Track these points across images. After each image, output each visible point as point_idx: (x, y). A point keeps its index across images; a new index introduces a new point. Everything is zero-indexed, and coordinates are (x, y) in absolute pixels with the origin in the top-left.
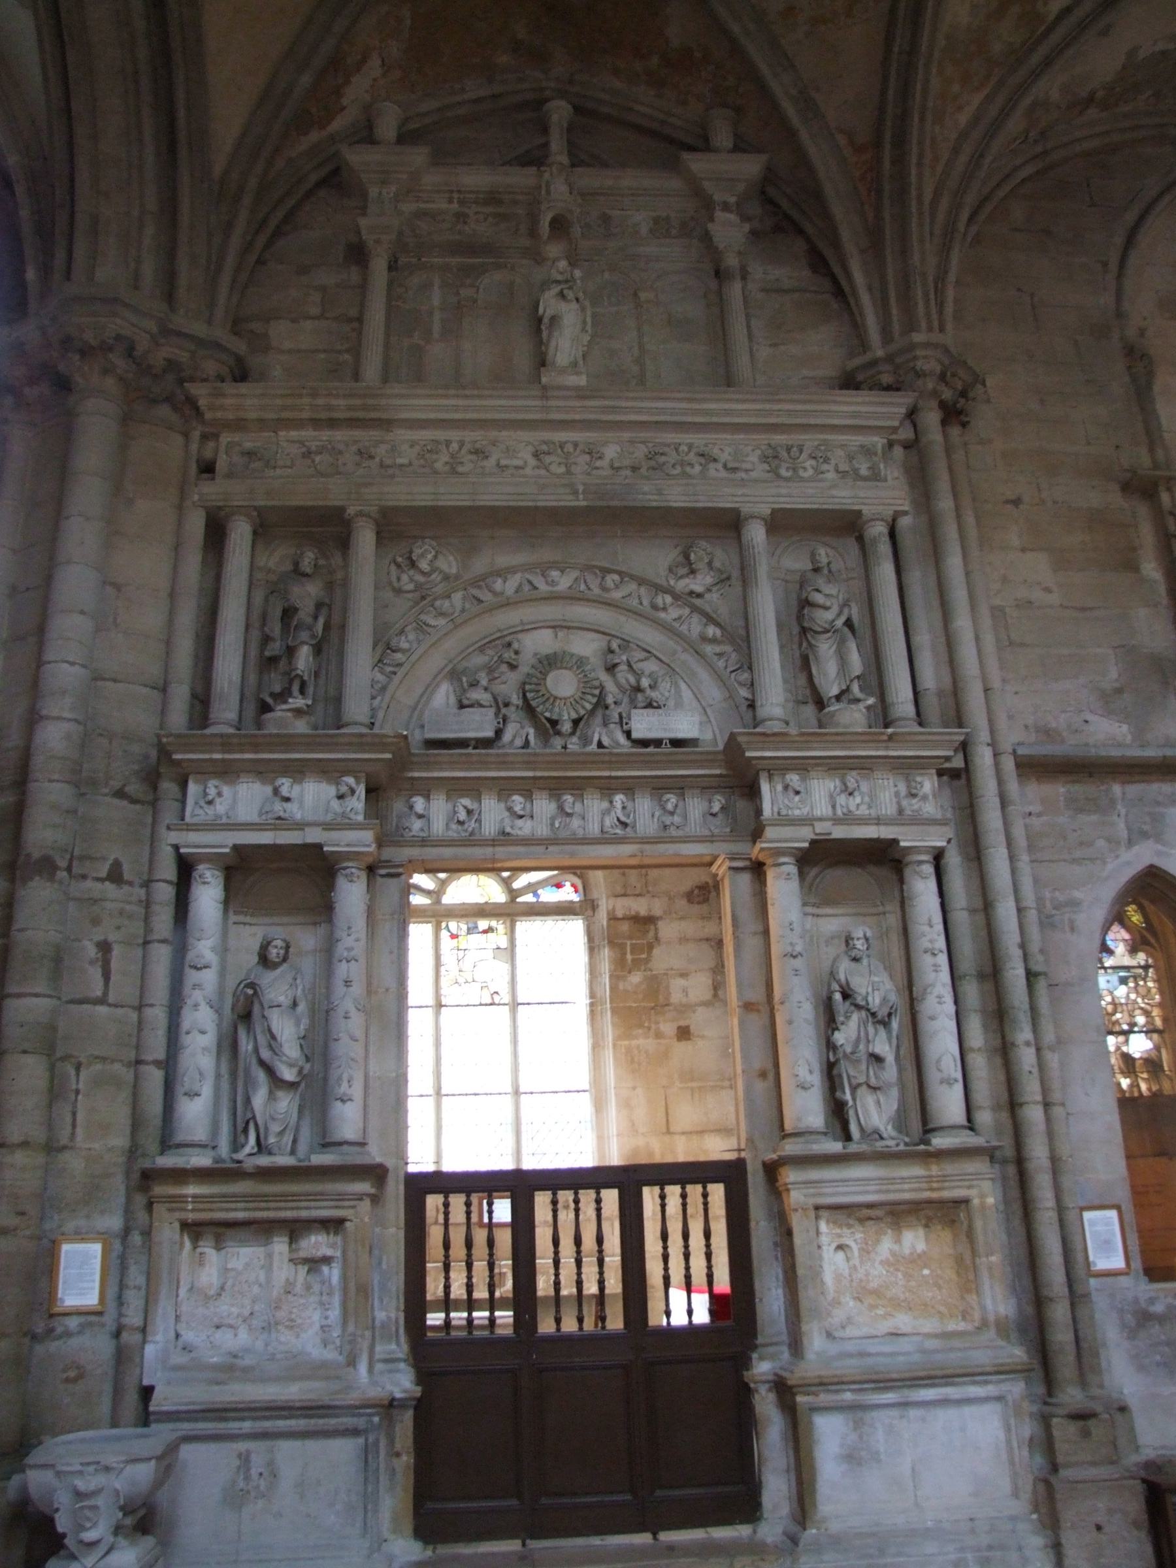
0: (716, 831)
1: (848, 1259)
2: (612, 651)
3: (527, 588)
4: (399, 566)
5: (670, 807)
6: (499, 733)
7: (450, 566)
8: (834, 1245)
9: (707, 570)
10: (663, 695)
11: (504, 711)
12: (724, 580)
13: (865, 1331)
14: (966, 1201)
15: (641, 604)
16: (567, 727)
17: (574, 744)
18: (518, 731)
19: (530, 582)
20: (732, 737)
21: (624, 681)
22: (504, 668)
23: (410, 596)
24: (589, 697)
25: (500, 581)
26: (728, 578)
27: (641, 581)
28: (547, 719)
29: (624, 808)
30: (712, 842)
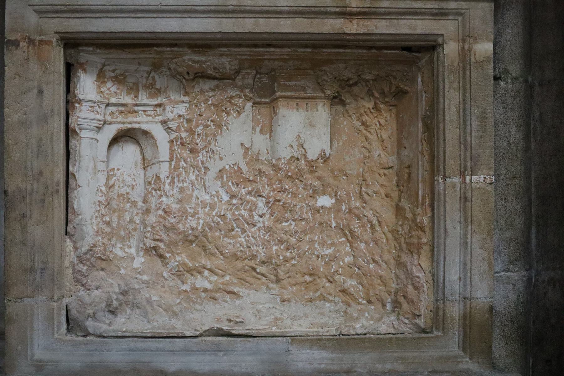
1: (146, 164)
8: (110, 131)
13: (161, 322)
14: (429, 47)
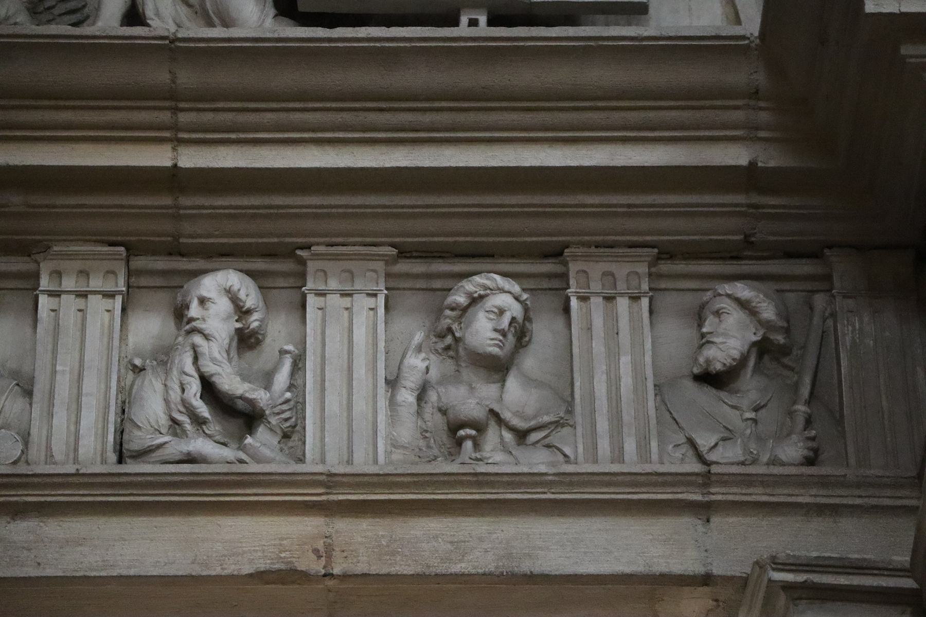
0: (727, 456)
5: (483, 332)
29: (246, 340)
30: (704, 510)
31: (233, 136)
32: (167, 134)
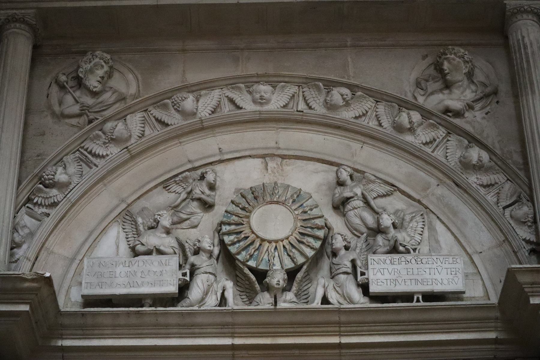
2: (341, 184)
3: (227, 108)
4: (62, 87)
6: (184, 288)
7: (128, 85)
9: (466, 82)
10: (412, 238)
11: (192, 259)
12: (490, 95)
15: (380, 125)
16: (277, 278)
17: (288, 301)
18: (212, 288)
19: (232, 101)
20: (511, 274)
21: (357, 221)
22: (194, 206)
23: (74, 121)
24: (311, 240)
25: (191, 98)
26: (495, 93)
27: (379, 97)
28: (251, 269)
31: (355, 333)
32: (338, 333)
